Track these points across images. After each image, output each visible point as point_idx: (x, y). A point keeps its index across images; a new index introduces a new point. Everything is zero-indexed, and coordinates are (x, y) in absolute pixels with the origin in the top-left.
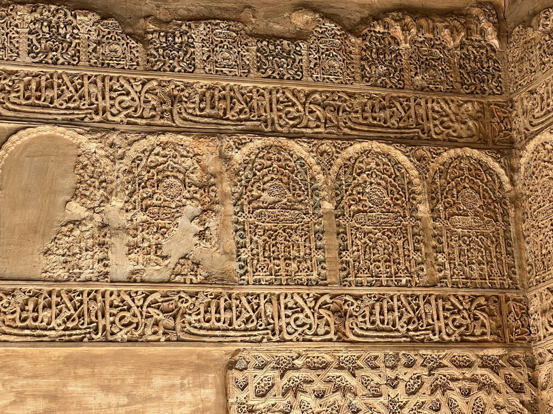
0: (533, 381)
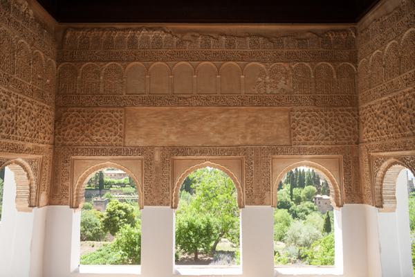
0: (358, 114)
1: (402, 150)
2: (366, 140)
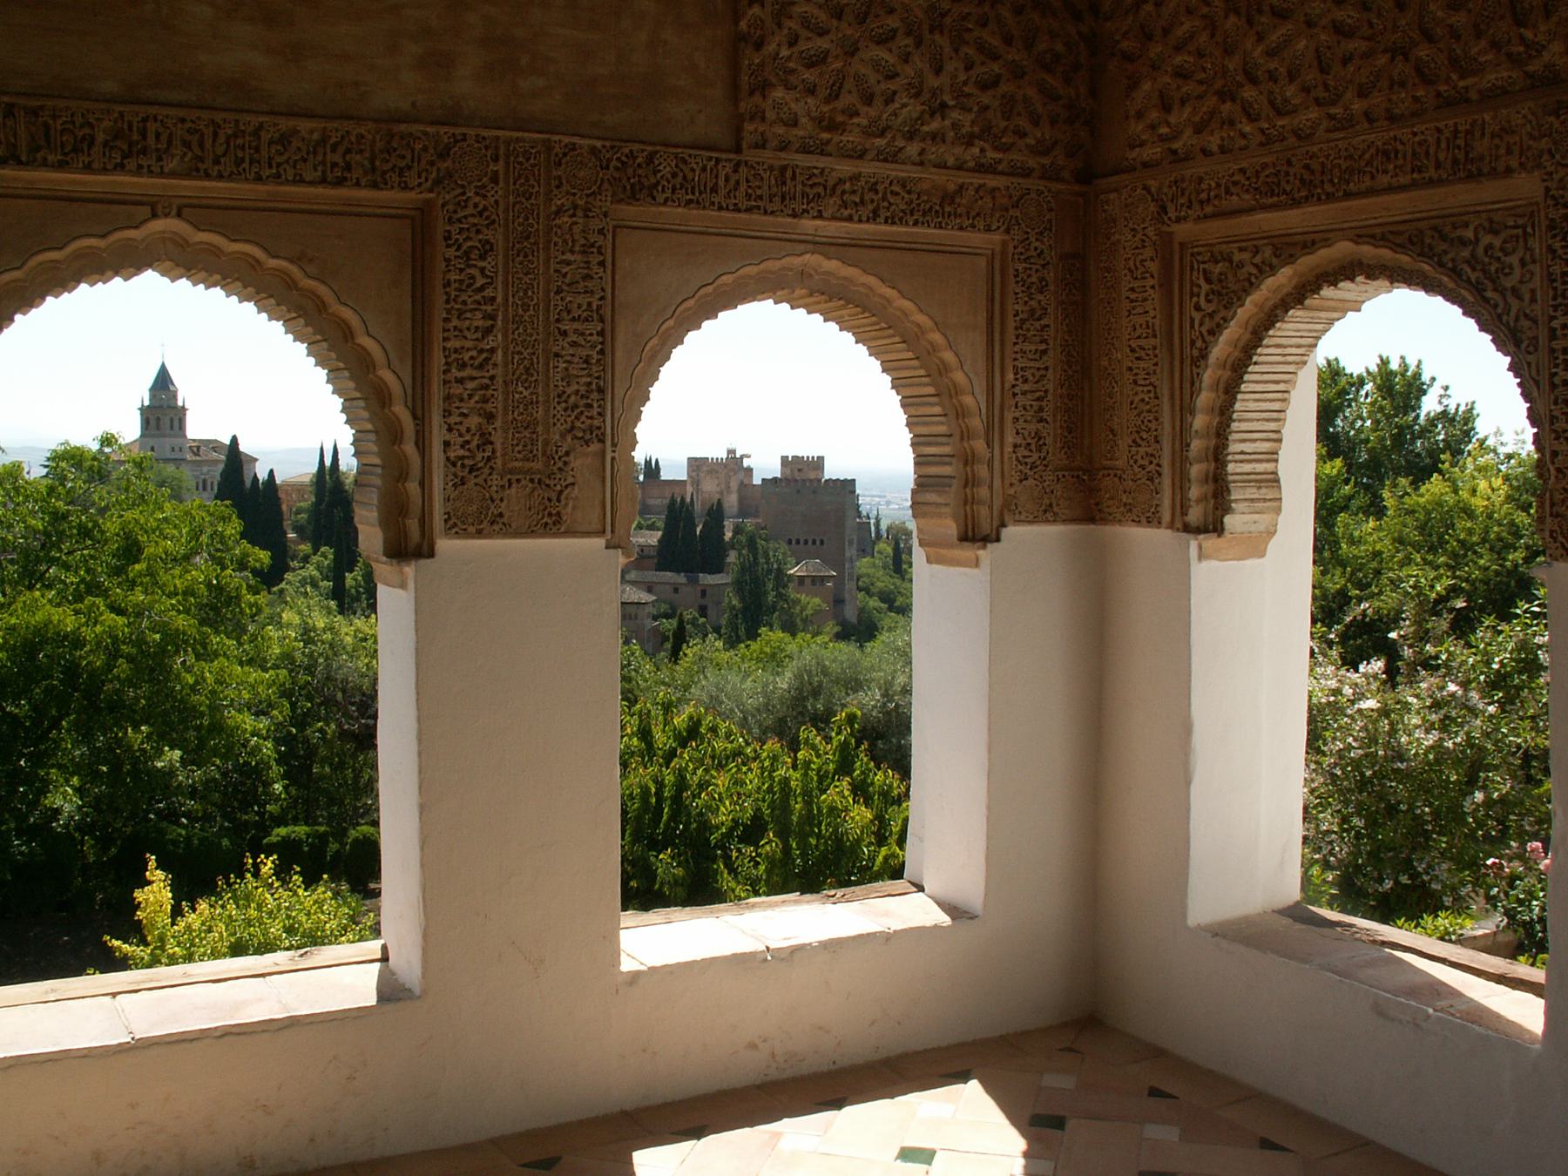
1: (1431, 183)
2: (1151, 152)
